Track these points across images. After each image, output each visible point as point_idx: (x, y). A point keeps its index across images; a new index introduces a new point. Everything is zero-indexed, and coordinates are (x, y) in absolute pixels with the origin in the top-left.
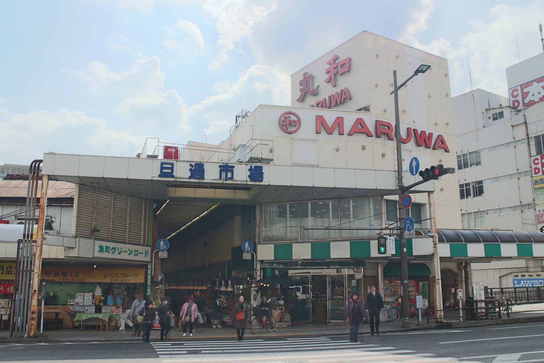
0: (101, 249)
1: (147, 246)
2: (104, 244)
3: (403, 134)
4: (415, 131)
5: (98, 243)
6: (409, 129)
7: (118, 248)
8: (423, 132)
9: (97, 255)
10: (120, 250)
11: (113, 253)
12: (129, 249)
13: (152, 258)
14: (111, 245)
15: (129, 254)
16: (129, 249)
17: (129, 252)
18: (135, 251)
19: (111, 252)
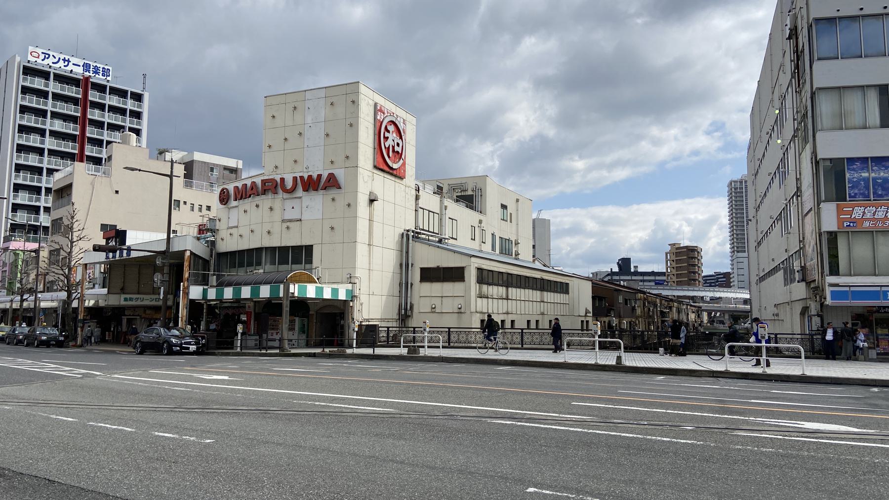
0: (126, 300)
1: (172, 294)
2: (128, 296)
3: (289, 184)
4: (302, 177)
5: (123, 296)
6: (295, 179)
7: (141, 298)
8: (310, 177)
9: (123, 303)
10: (142, 299)
11: (136, 301)
12: (151, 299)
13: (174, 302)
14: (134, 296)
15: (151, 301)
16: (151, 299)
17: (151, 300)
18: (156, 299)
19: (134, 300)
